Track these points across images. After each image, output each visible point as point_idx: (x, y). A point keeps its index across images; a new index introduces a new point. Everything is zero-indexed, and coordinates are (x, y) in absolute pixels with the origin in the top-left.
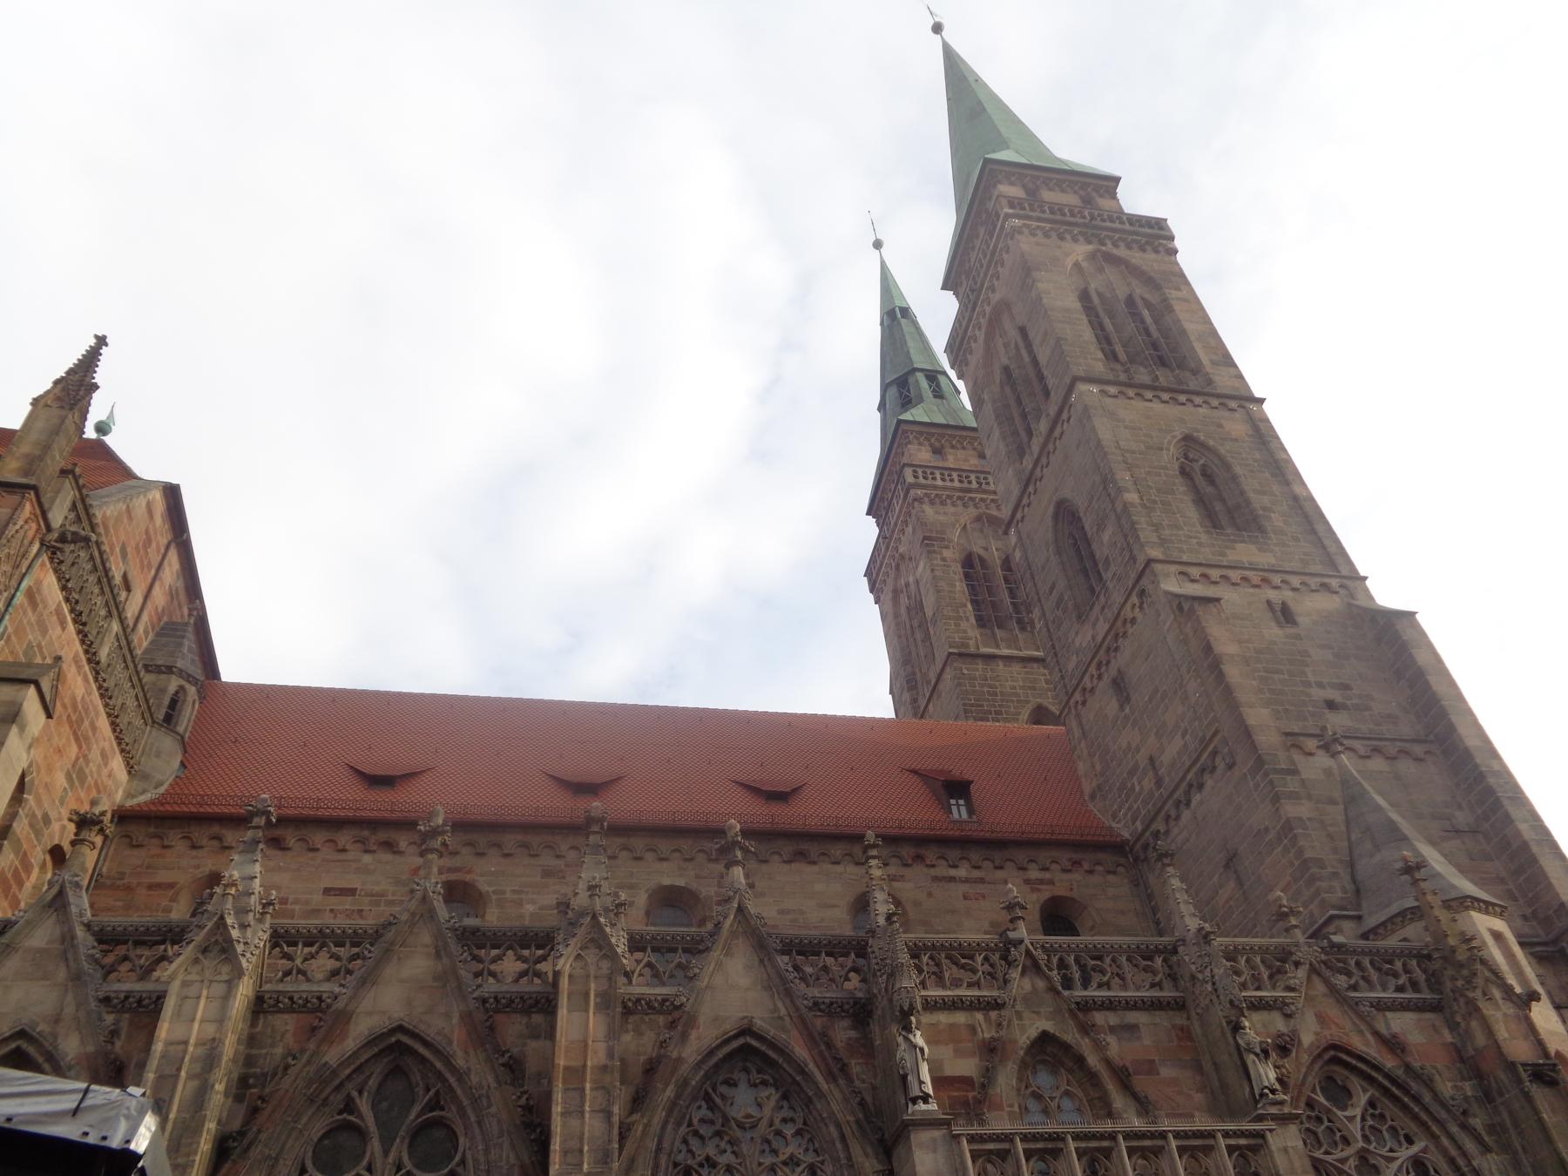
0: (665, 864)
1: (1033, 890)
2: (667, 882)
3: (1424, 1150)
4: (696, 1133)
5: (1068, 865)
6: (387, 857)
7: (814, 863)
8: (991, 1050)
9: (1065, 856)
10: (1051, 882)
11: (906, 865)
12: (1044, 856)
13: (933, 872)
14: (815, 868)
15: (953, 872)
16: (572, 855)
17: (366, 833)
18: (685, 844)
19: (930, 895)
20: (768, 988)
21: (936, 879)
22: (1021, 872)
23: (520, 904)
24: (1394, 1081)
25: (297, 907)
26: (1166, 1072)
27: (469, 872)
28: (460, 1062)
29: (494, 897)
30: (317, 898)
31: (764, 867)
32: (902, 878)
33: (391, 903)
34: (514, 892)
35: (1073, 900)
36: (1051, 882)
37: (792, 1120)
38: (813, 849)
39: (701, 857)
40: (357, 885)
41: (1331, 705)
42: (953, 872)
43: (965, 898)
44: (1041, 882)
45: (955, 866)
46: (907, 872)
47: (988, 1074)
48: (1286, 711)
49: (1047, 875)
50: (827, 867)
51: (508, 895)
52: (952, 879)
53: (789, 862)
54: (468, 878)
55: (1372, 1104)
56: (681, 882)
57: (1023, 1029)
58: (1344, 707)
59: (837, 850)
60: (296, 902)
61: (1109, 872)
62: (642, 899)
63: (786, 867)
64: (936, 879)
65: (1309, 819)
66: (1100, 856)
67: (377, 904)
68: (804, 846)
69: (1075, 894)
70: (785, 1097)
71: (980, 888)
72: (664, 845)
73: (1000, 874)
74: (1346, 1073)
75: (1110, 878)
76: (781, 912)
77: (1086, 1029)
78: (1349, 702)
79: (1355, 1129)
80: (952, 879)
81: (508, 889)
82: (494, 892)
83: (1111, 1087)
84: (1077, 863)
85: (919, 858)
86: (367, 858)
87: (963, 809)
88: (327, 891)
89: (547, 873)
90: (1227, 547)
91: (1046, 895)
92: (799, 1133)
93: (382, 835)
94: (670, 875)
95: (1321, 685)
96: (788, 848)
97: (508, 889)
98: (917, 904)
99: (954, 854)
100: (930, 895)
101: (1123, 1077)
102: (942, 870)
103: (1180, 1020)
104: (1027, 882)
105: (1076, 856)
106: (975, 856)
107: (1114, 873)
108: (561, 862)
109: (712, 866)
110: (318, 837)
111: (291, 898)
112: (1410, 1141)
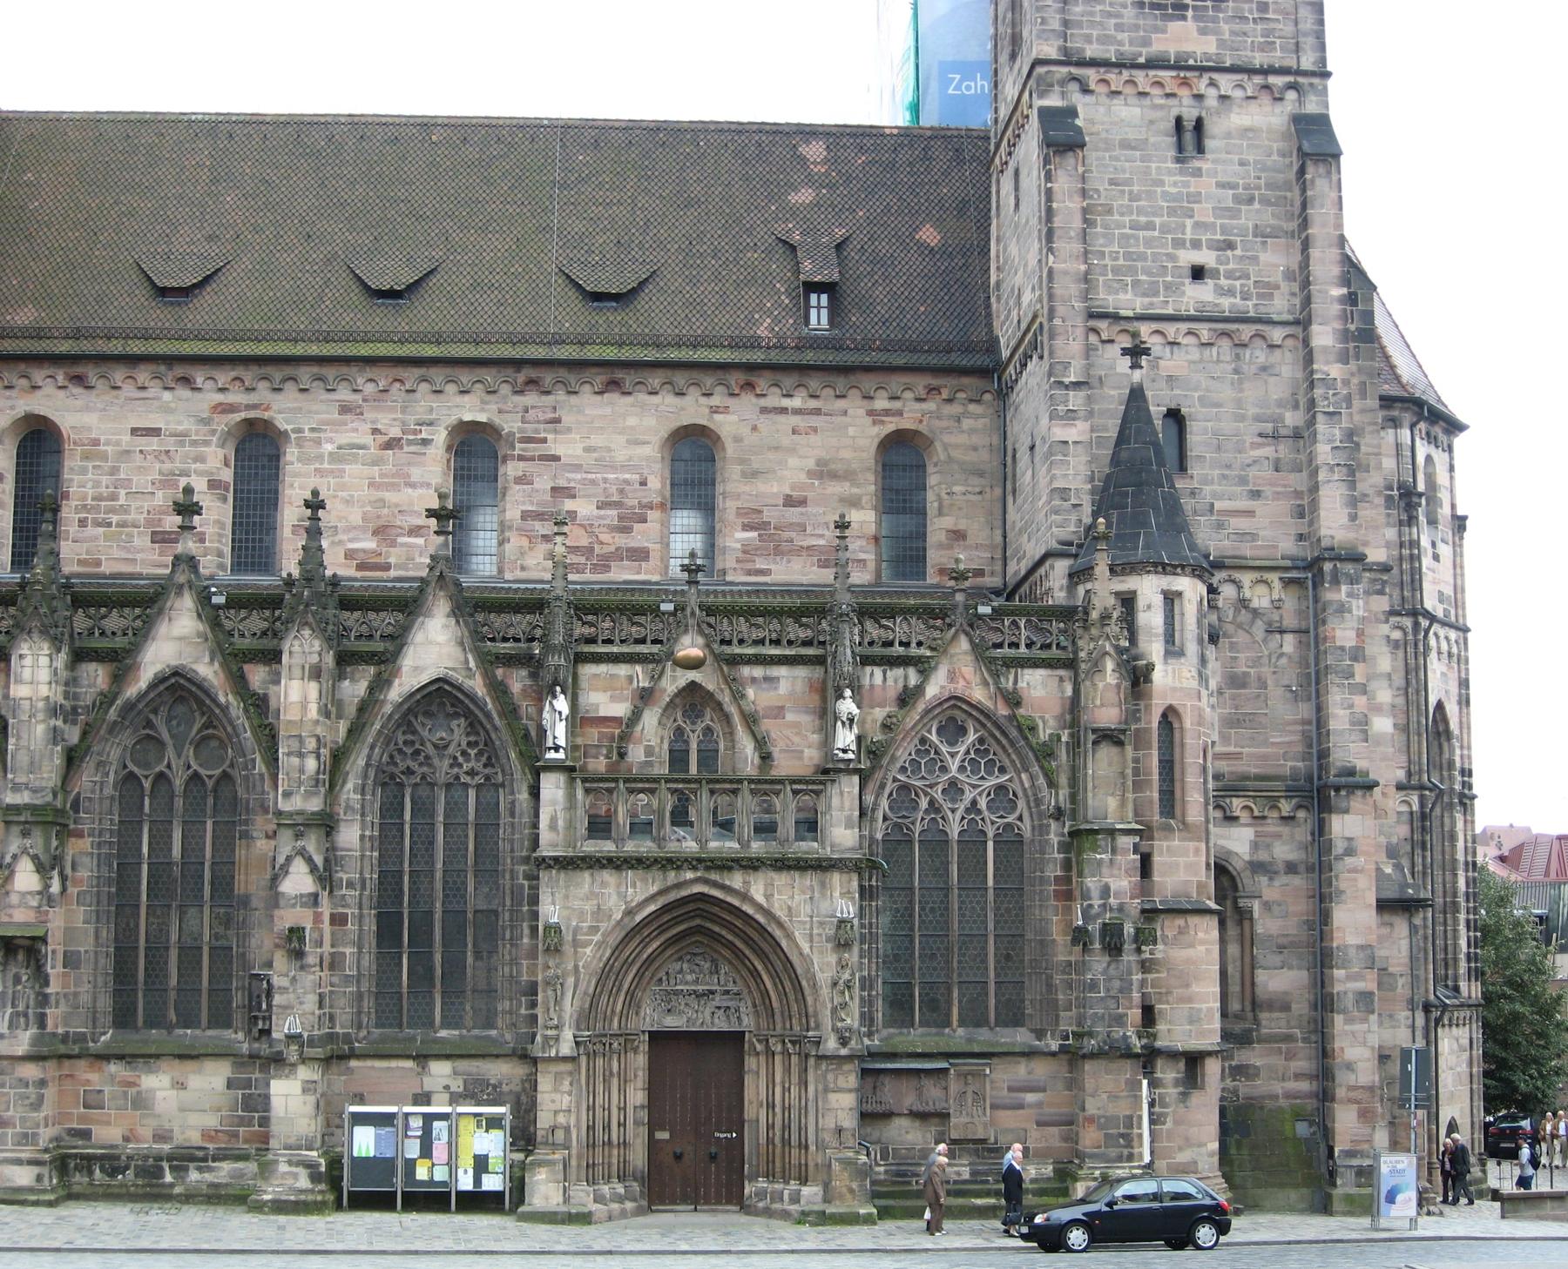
0: (467, 398)
1: (874, 423)
2: (467, 417)
3: (1010, 780)
4: (400, 751)
5: (922, 393)
6: (184, 393)
7: (629, 393)
8: (645, 697)
9: (921, 382)
10: (900, 413)
11: (732, 395)
12: (896, 382)
13: (763, 402)
14: (629, 400)
15: (786, 402)
16: (369, 388)
17: (162, 368)
18: (489, 375)
19: (754, 428)
20: (461, 644)
21: (764, 410)
22: (866, 402)
23: (318, 442)
24: (999, 728)
25: (109, 448)
26: (790, 717)
27: (266, 409)
28: (222, 699)
29: (293, 436)
30: (126, 438)
31: (573, 399)
32: (726, 410)
33: (194, 443)
34: (312, 430)
35: (916, 432)
36: (900, 413)
37: (476, 743)
38: (628, 378)
39: (505, 389)
40: (161, 425)
41: (1198, 273)
42: (786, 402)
43: (794, 432)
44: (887, 412)
45: (789, 396)
46: (731, 402)
47: (636, 716)
48: (1136, 283)
49: (897, 405)
50: (642, 397)
51: (307, 434)
52: (784, 410)
53: (601, 393)
54: (266, 415)
55: (981, 741)
56: (482, 418)
57: (674, 678)
58: (1215, 274)
59: (655, 380)
60: (107, 443)
61: (971, 401)
62: (441, 437)
63: (599, 398)
64: (764, 410)
65: (1075, 443)
66: (966, 381)
67: (182, 444)
68: (619, 374)
69: (922, 428)
70: (471, 725)
71: (815, 421)
72: (465, 376)
73: (841, 404)
74: (964, 716)
75: (972, 407)
76: (587, 450)
77: (730, 681)
78: (1222, 268)
79: (954, 766)
80: (784, 410)
81: (306, 428)
82: (294, 431)
83: (740, 730)
84: (937, 390)
85: (749, 386)
86: (167, 396)
87: (824, 313)
88: (134, 431)
89: (345, 409)
90: (1157, 30)
91: (890, 428)
92: (480, 753)
93: (180, 371)
94: (472, 410)
95: (1196, 245)
96: (600, 379)
97: (306, 428)
98: (738, 439)
99: (789, 381)
100: (754, 428)
101: (751, 720)
102: (774, 399)
103: (817, 672)
104: (871, 413)
105: (935, 382)
106: (814, 383)
107: (978, 401)
108: (358, 397)
109: (518, 399)
110: (119, 374)
111: (103, 438)
112: (1002, 770)
